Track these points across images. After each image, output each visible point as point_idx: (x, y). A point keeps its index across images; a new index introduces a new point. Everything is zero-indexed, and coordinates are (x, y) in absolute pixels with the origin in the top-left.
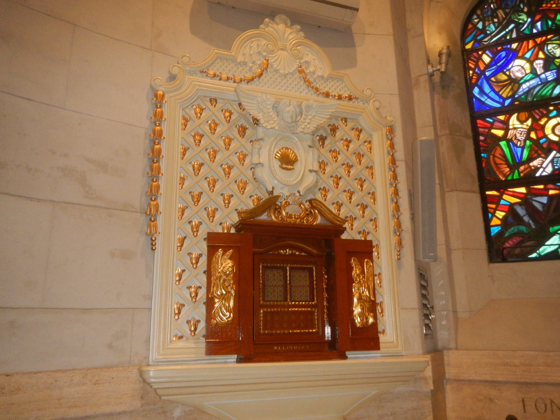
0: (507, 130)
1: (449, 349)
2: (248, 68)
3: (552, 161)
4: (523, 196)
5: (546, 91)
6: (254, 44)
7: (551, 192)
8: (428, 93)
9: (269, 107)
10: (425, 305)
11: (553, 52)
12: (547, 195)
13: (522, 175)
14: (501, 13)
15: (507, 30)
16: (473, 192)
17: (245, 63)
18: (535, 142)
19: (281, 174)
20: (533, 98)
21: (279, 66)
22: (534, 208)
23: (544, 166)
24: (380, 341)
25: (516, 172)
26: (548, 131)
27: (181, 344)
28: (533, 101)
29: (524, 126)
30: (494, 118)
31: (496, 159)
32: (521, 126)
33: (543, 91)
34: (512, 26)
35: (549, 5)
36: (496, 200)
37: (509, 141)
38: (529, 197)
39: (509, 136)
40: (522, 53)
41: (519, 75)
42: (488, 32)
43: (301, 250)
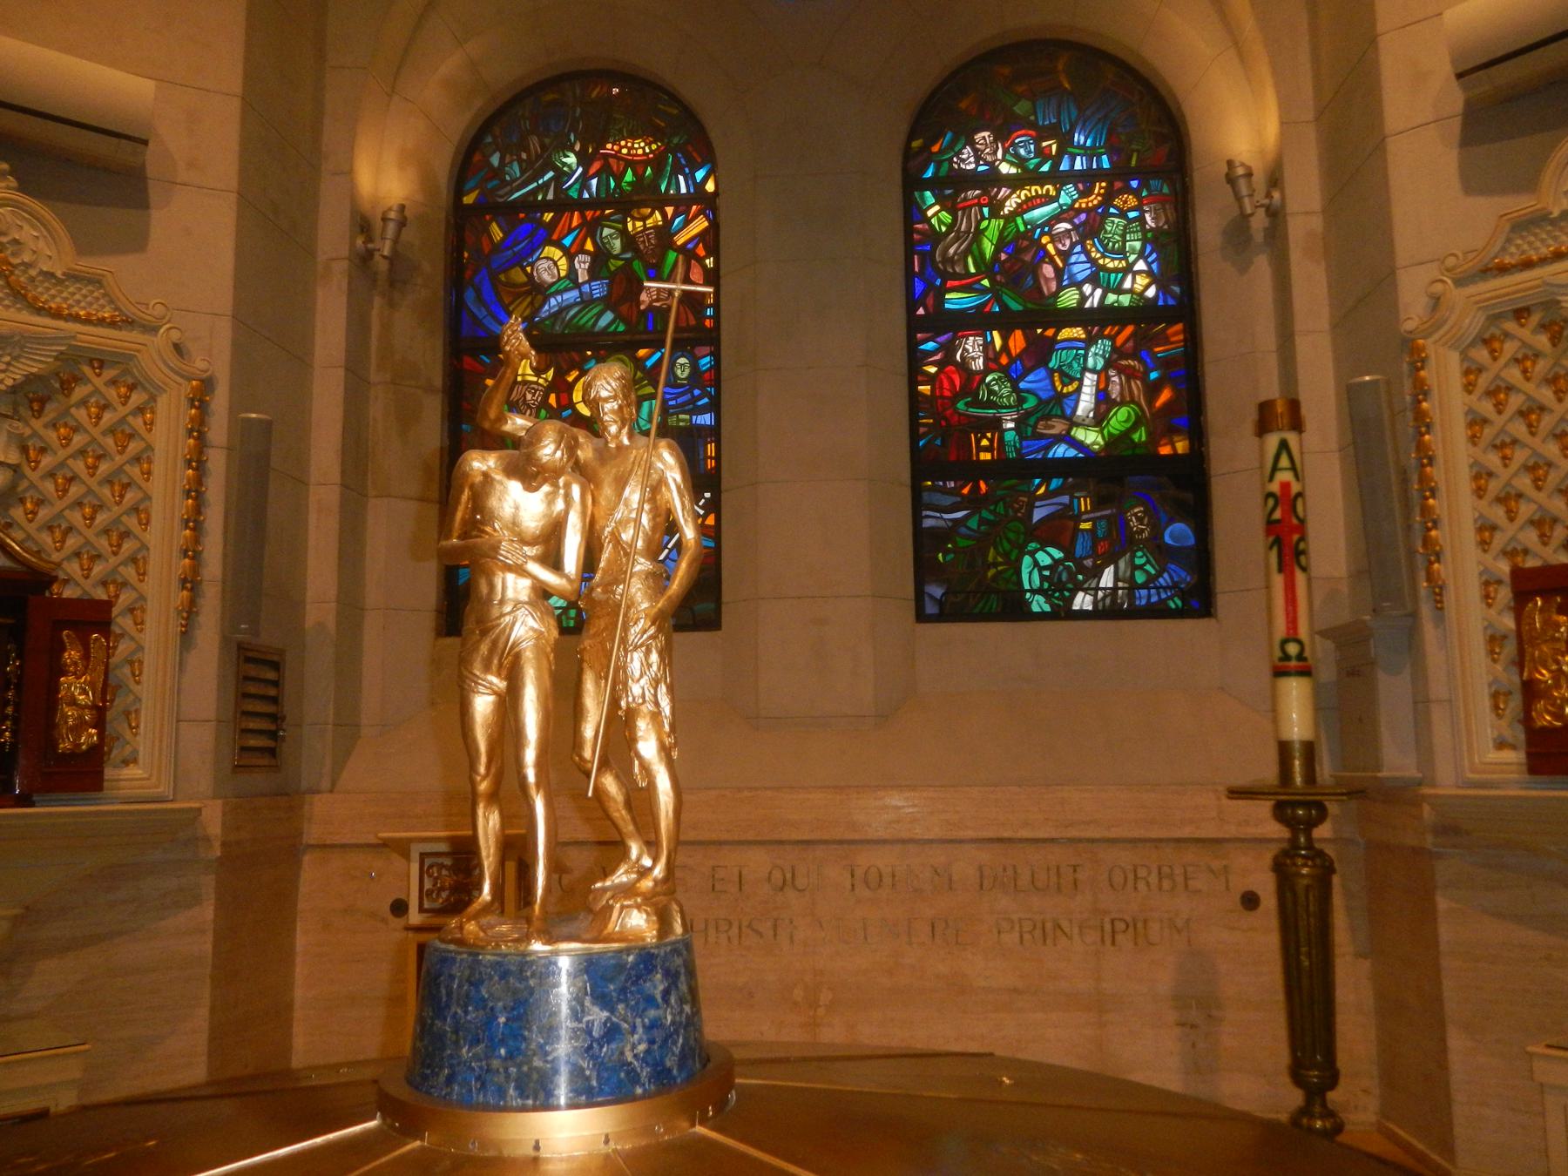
1: (319, 792)
5: (586, 319)
14: (534, 143)
15: (540, 182)
20: (564, 329)
24: (106, 777)
28: (563, 335)
29: (541, 381)
32: (535, 379)
33: (581, 318)
34: (551, 174)
40: (560, 233)
41: (547, 278)
42: (508, 178)
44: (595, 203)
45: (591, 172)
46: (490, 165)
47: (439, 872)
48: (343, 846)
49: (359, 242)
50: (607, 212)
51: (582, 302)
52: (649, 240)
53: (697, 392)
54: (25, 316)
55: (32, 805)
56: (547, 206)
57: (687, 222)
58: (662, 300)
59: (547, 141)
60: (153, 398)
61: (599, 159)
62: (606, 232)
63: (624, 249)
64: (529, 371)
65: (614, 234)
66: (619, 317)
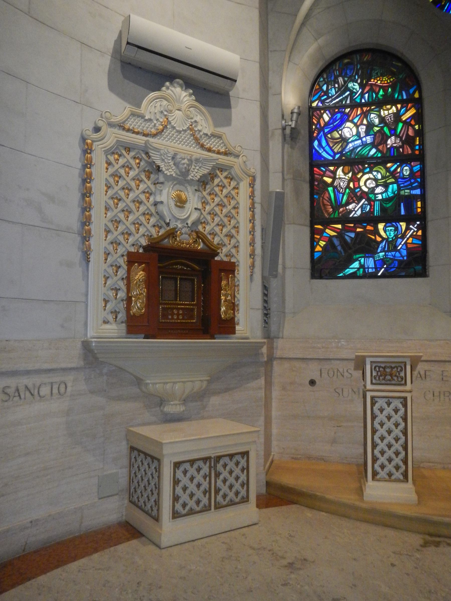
0: (334, 178)
1: (278, 338)
2: (153, 124)
3: (361, 207)
4: (339, 231)
5: (365, 151)
6: (159, 104)
7: (358, 230)
8: (281, 144)
9: (169, 158)
10: (265, 307)
11: (373, 120)
12: (355, 231)
13: (340, 215)
14: (341, 80)
15: (344, 96)
16: (305, 226)
17: (150, 120)
18: (352, 191)
19: (176, 212)
20: (356, 156)
21: (176, 124)
22: (345, 241)
23: (356, 209)
24: (236, 329)
25: (337, 212)
26: (362, 183)
27: (107, 326)
28: (355, 158)
29: (347, 178)
30: (326, 168)
31: (324, 201)
32: (344, 177)
34: (348, 93)
35: (376, 81)
36: (321, 232)
37: (335, 188)
38: (343, 232)
39: (335, 184)
40: (353, 117)
41: (348, 135)
42: (330, 95)
43: (188, 266)
44: (367, 104)
45: (365, 91)
46: (323, 90)
47: (379, 369)
48: (290, 359)
49: (283, 122)
50: (372, 107)
51: (363, 145)
52: (391, 119)
53: (412, 181)
54: (200, 151)
55: (215, 339)
56: (346, 106)
57: (407, 111)
58: (397, 143)
59: (346, 79)
60: (238, 184)
61: (368, 86)
62: (372, 116)
63: (380, 123)
64: (341, 173)
65: (376, 116)
66: (378, 150)
